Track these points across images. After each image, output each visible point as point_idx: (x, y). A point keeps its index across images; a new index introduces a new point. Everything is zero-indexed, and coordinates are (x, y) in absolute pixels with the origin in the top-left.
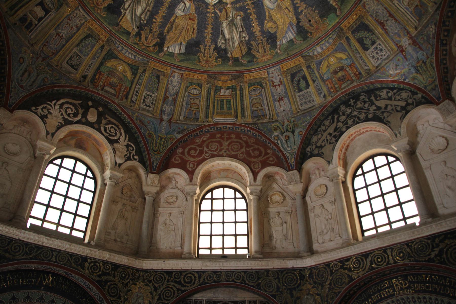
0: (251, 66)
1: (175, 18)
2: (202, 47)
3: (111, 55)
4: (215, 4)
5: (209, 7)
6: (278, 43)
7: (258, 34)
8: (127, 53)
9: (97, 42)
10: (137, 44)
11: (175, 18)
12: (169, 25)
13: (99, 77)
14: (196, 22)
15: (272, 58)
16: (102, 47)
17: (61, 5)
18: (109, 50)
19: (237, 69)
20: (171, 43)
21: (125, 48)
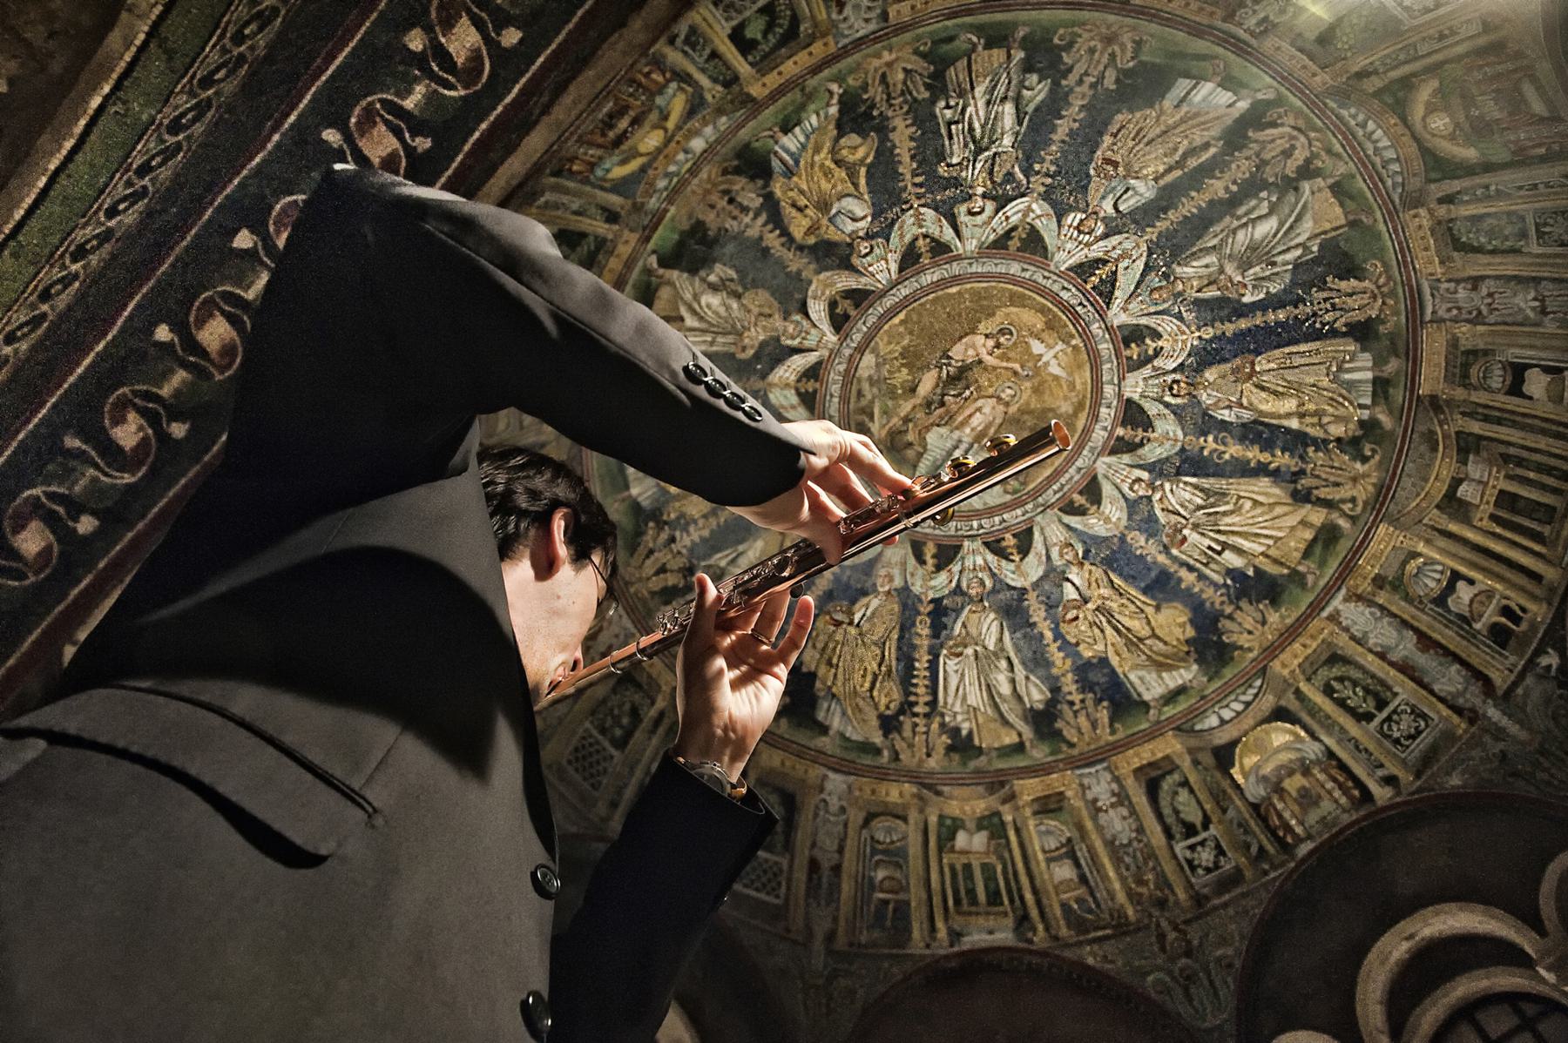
0: (947, 28)
1: (1163, 175)
2: (1110, 82)
3: (1439, 166)
4: (1023, 195)
5: (1042, 189)
6: (833, 110)
7: (899, 123)
8: (1380, 145)
9: (1451, 220)
10: (1329, 151)
11: (1163, 175)
12: (1193, 163)
13: (1534, 147)
14: (1099, 153)
15: (859, 64)
16: (1448, 200)
17: (1473, 353)
18: (1435, 181)
19: (999, 17)
20: (1211, 116)
21: (1377, 160)
